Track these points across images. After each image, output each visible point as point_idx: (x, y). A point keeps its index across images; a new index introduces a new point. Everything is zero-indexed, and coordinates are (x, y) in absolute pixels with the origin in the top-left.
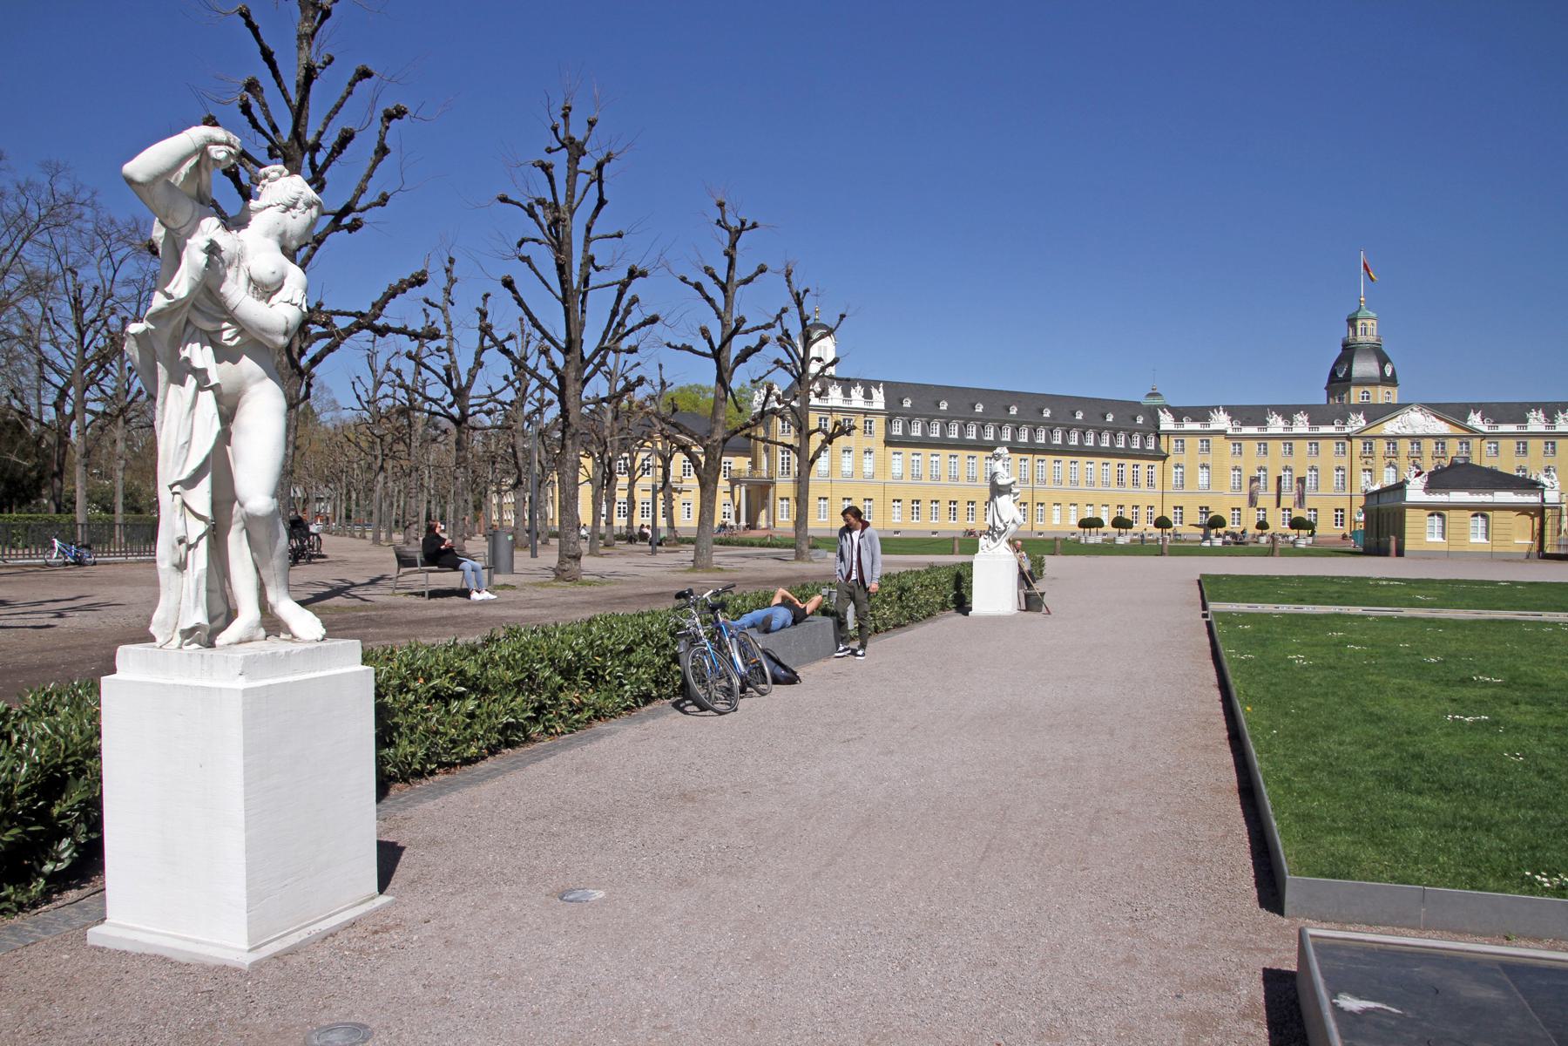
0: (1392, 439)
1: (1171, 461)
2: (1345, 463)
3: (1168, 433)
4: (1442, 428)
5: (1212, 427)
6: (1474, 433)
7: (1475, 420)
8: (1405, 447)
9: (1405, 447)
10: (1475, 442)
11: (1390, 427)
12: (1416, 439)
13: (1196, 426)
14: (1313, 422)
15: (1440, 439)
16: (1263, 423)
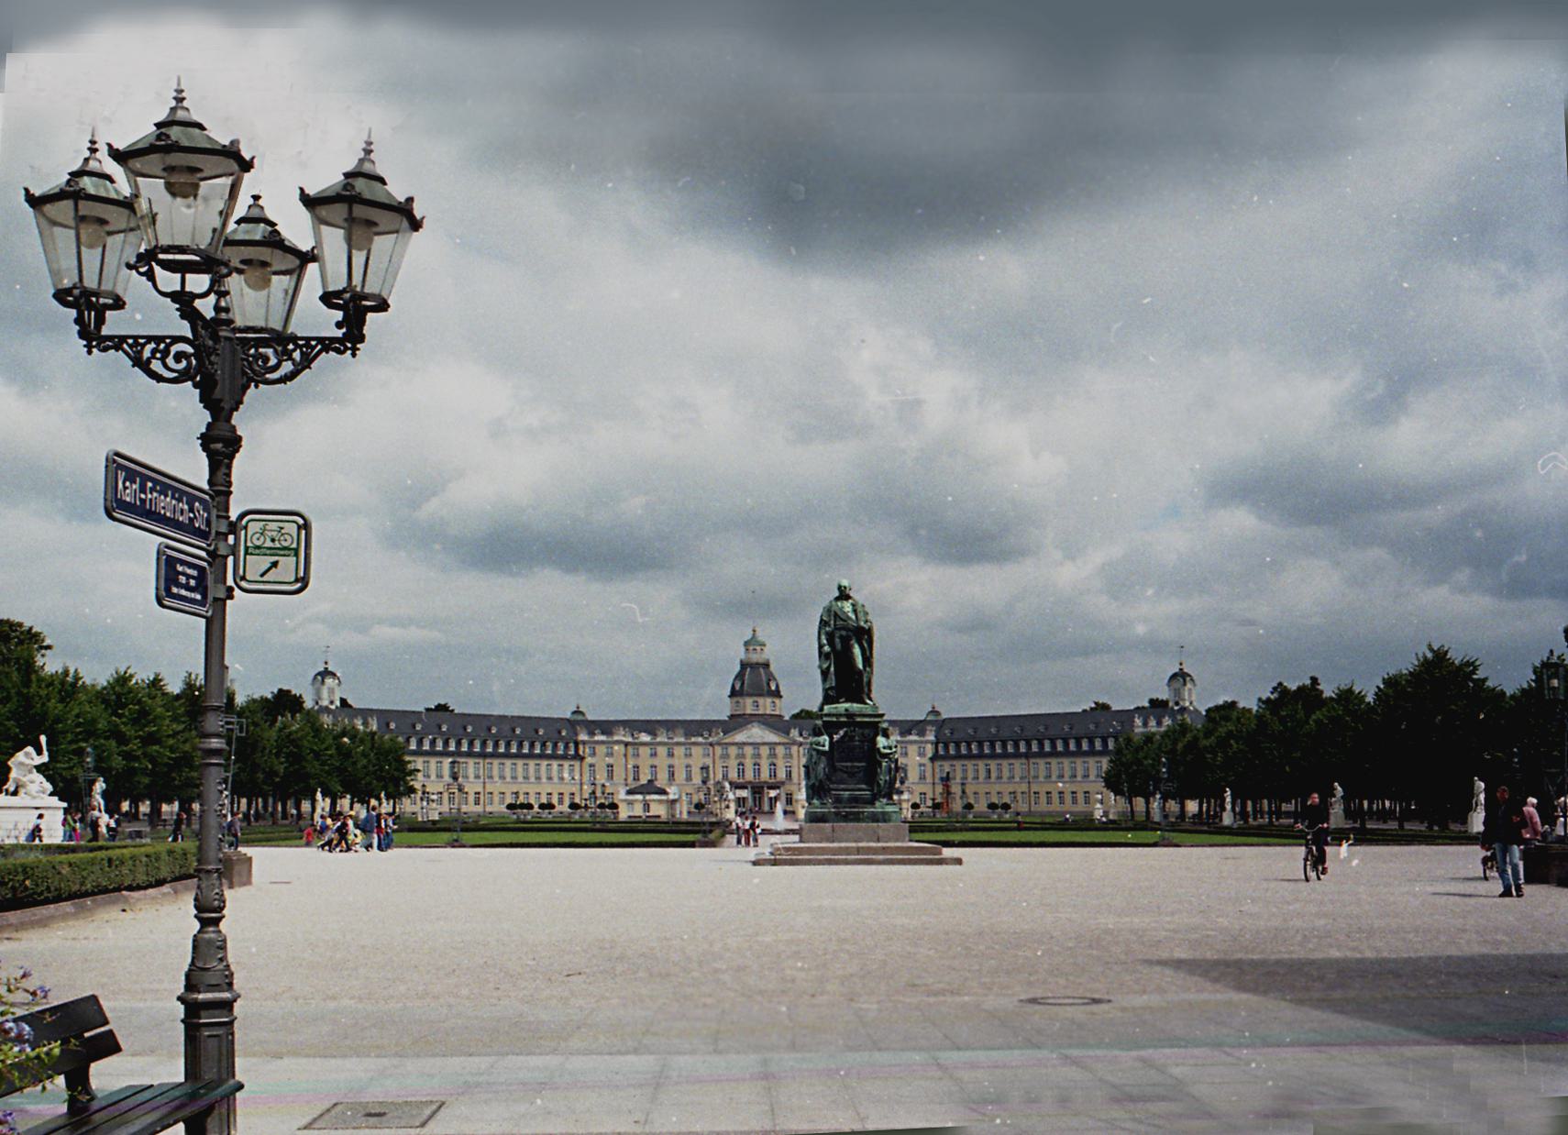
0: (741, 745)
1: (589, 760)
2: (709, 761)
3: (584, 743)
4: (772, 737)
5: (616, 738)
6: (794, 743)
7: (794, 733)
8: (749, 751)
9: (749, 751)
10: (795, 748)
11: (740, 737)
12: (756, 745)
13: (603, 738)
14: (687, 735)
15: (772, 745)
16: (654, 734)
